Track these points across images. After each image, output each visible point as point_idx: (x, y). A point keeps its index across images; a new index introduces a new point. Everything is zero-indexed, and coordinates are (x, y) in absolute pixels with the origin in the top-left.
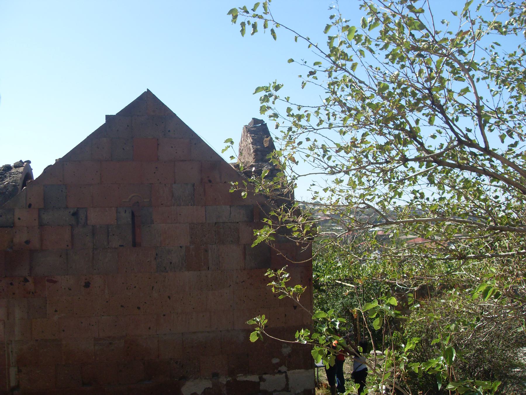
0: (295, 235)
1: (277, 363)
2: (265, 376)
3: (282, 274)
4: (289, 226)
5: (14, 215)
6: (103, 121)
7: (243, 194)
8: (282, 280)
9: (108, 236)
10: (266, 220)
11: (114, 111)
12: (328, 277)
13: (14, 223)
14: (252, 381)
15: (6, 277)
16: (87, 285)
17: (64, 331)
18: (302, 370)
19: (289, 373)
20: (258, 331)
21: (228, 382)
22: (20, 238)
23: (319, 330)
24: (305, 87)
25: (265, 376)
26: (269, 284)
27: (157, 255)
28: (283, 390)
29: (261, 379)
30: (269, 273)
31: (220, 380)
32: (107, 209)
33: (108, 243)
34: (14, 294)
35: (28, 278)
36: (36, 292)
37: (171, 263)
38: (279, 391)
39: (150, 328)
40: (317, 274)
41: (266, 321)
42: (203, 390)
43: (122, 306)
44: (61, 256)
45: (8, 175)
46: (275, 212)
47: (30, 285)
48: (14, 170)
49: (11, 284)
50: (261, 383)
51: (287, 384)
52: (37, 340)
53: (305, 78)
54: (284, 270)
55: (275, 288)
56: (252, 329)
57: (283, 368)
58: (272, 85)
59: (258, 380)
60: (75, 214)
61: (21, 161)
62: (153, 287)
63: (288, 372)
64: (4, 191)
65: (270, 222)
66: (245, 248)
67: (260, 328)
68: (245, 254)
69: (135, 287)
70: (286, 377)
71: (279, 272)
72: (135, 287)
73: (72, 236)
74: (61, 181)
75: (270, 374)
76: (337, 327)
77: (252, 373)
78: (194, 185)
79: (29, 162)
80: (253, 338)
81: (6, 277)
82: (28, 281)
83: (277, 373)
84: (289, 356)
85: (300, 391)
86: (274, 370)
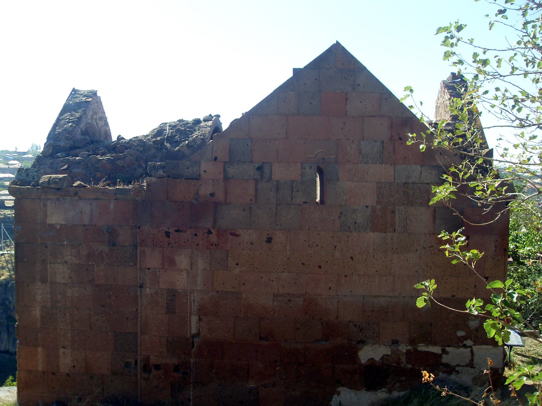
0: (478, 194)
2: (448, 349)
3: (458, 237)
4: (472, 184)
5: (200, 167)
6: (290, 75)
7: (421, 147)
8: (457, 243)
9: (292, 192)
10: (445, 176)
11: (301, 65)
12: (528, 248)
13: (200, 176)
14: (433, 353)
15: (190, 227)
17: (244, 284)
19: (475, 348)
20: (425, 296)
21: (408, 351)
22: (205, 191)
23: (493, 301)
24: (493, 28)
25: (448, 349)
26: (442, 247)
27: (341, 214)
28: (467, 366)
30: (443, 235)
31: (400, 348)
32: (292, 164)
33: (292, 199)
34: (198, 245)
36: (218, 244)
37: (355, 223)
38: (463, 366)
39: (330, 288)
40: (516, 245)
41: (435, 286)
42: (381, 357)
43: (303, 264)
44: (244, 210)
45: (197, 128)
46: (456, 168)
47: (213, 238)
48: (203, 124)
49: (196, 235)
51: (472, 360)
52: (218, 292)
53: (493, 18)
54: (460, 233)
55: (449, 252)
56: (419, 293)
57: (469, 342)
58: (454, 25)
59: (440, 352)
60: (259, 169)
61: (210, 115)
62: (335, 247)
63: (473, 347)
64: (193, 144)
65: (450, 179)
66: (435, 211)
67: (428, 292)
68: (434, 218)
69: (317, 245)
71: (454, 235)
72: (317, 245)
73: (256, 190)
74: (246, 135)
76: (515, 300)
77: (435, 344)
78: (383, 143)
79: (218, 116)
80: (420, 303)
81: (190, 227)
82: (212, 233)
86: (459, 343)
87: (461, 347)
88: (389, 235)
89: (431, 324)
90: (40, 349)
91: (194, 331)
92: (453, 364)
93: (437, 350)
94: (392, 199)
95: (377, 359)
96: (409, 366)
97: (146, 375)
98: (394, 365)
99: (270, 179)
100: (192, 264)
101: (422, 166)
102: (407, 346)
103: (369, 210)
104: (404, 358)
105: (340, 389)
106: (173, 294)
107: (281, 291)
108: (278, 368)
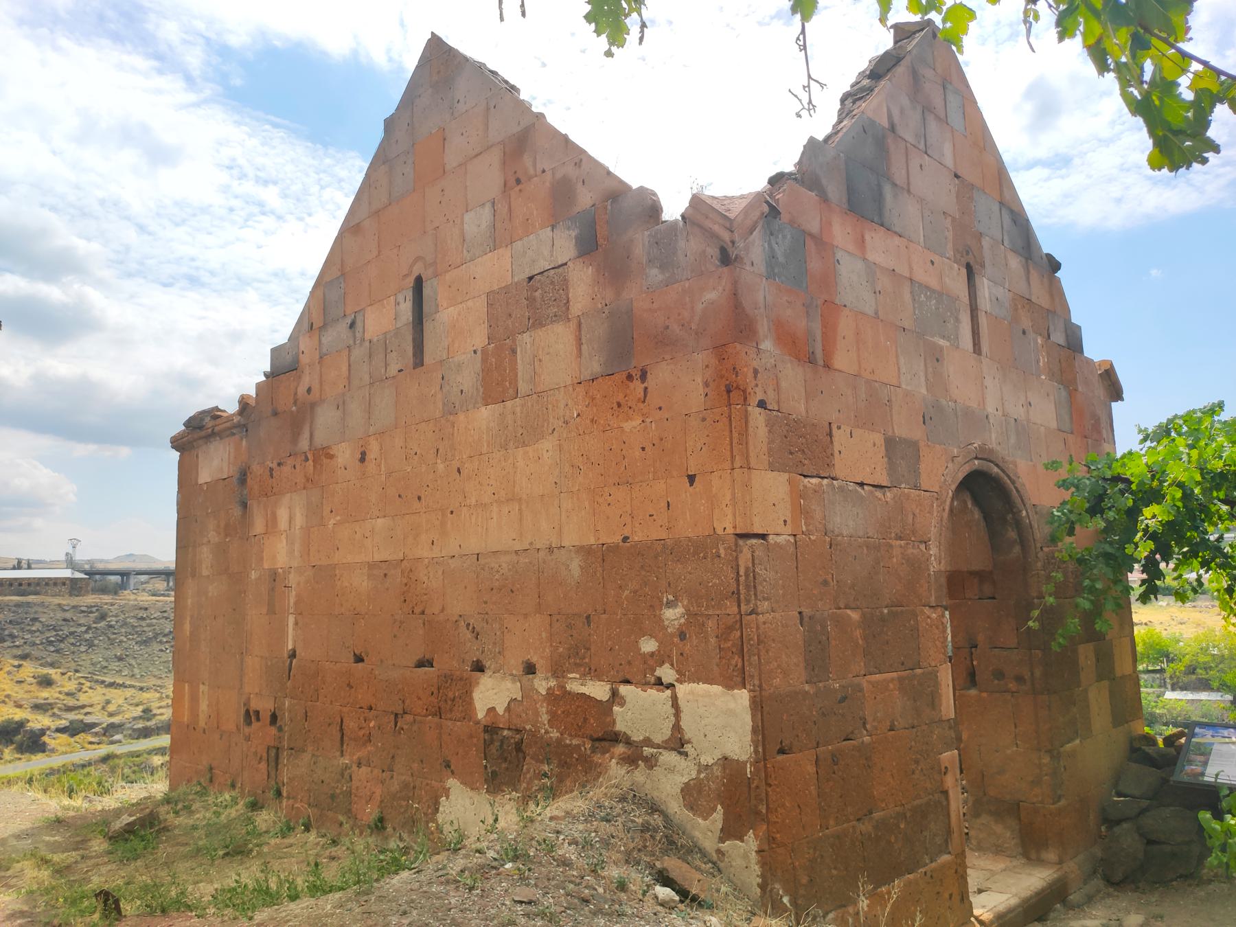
1: (652, 654)
13: (298, 362)
18: (716, 689)
19: (682, 690)
25: (624, 689)
29: (614, 693)
35: (309, 456)
38: (658, 747)
50: (616, 709)
51: (677, 727)
60: (352, 325)
66: (580, 324)
68: (579, 343)
70: (674, 699)
75: (636, 685)
84: (682, 636)
85: (711, 762)
87: (647, 683)
88: (509, 404)
89: (588, 617)
91: (290, 647)
92: (637, 737)
93: (598, 690)
94: (509, 322)
95: (500, 710)
96: (555, 734)
97: (247, 730)
98: (528, 727)
99: (363, 340)
100: (291, 519)
101: (553, 227)
103: (479, 353)
104: (544, 710)
105: (452, 783)
106: (274, 575)
107: (377, 557)
108: (372, 725)
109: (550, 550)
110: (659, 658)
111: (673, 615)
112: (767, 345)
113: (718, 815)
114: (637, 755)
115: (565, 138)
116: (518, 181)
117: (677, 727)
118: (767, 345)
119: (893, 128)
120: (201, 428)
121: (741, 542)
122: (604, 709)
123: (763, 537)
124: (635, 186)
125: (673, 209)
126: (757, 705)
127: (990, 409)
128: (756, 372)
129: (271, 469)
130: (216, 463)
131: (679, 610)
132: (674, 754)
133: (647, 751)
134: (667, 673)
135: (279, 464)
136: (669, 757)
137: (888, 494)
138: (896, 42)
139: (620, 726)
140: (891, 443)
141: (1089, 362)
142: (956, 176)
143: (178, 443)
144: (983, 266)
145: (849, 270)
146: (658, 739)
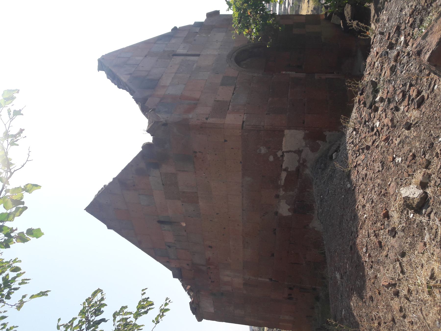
1: (274, 157)
16: (211, 247)
19: (284, 149)
21: (283, 190)
31: (281, 194)
38: (300, 158)
50: (289, 170)
51: (295, 152)
57: (279, 154)
60: (169, 247)
63: (284, 149)
77: (279, 175)
83: (283, 158)
85: (304, 143)
90: (280, 324)
91: (268, 280)
92: (297, 164)
93: (284, 175)
96: (296, 190)
101: (149, 176)
102: (280, 191)
105: (311, 226)
109: (242, 186)
110: (275, 156)
111: (263, 150)
112: (190, 116)
113: (319, 142)
114: (303, 164)
115: (123, 170)
116: (134, 186)
117: (295, 152)
118: (190, 116)
119: (130, 74)
120: (196, 309)
121: (244, 128)
122: (290, 174)
123: (243, 122)
124: (141, 149)
125: (149, 139)
126: (289, 128)
127: (216, 53)
128: (198, 120)
129: (212, 282)
130: (208, 305)
131: (262, 148)
132: (302, 154)
133: (301, 162)
134: (279, 154)
135: (210, 279)
136: (303, 155)
137: (237, 86)
138: (103, 70)
139: (294, 169)
140: (222, 84)
141: (206, 20)
142: (146, 56)
143: (200, 320)
144: (173, 51)
145: (171, 91)
146: (298, 158)
